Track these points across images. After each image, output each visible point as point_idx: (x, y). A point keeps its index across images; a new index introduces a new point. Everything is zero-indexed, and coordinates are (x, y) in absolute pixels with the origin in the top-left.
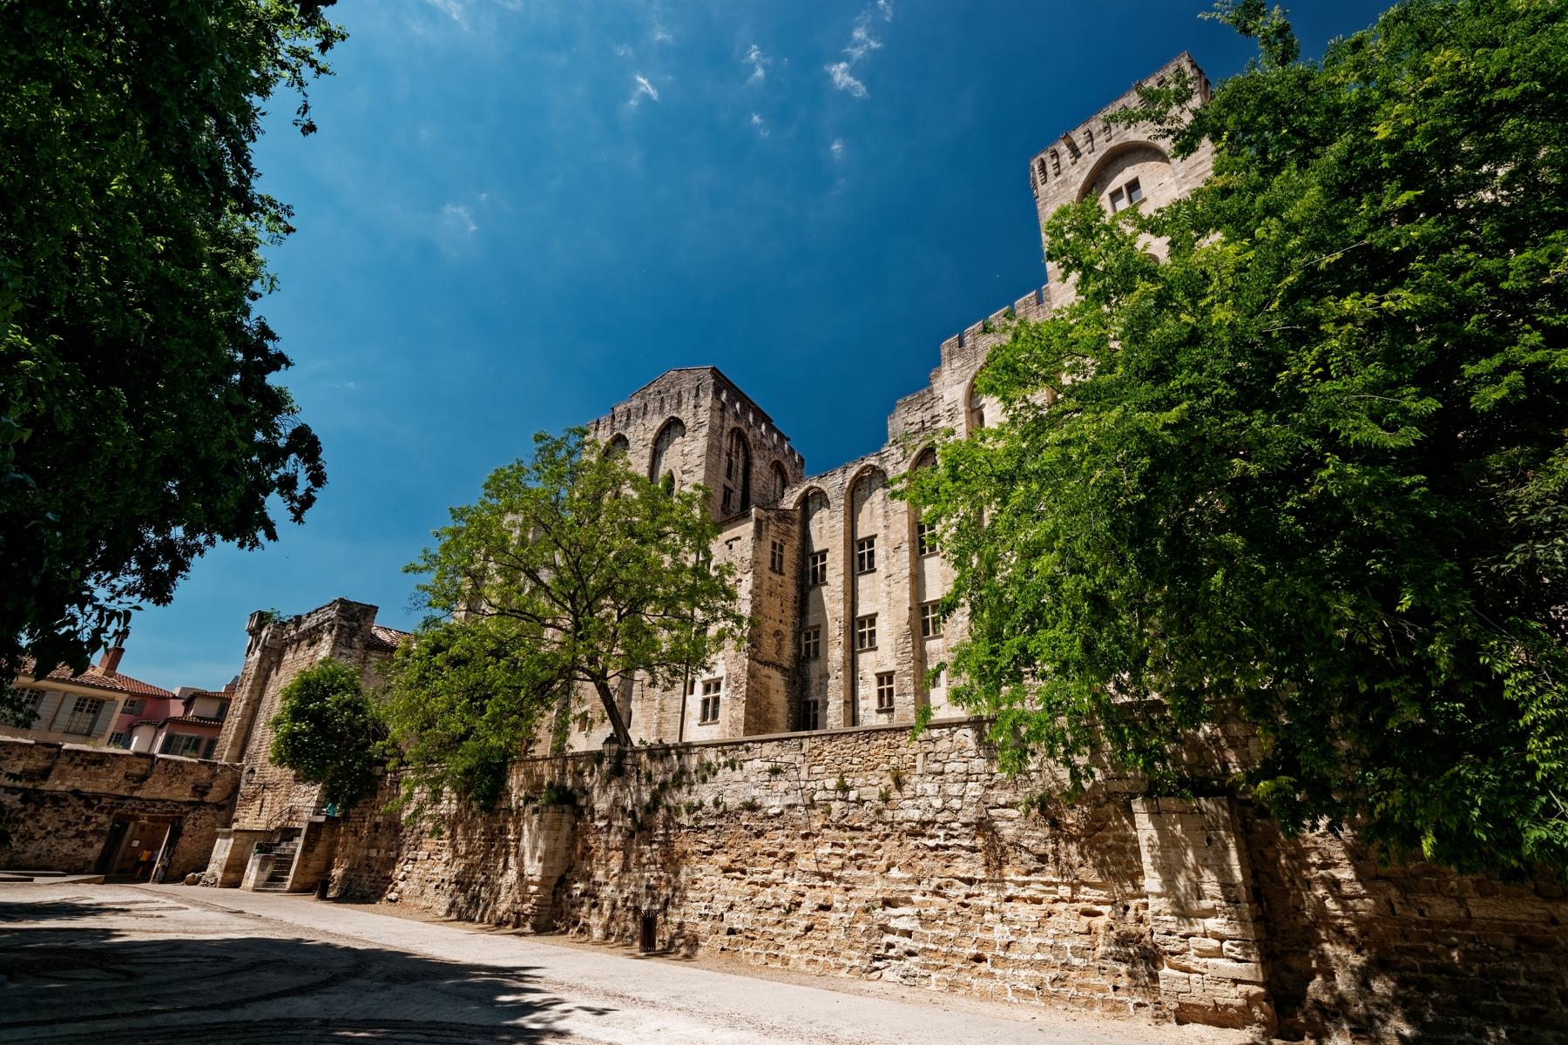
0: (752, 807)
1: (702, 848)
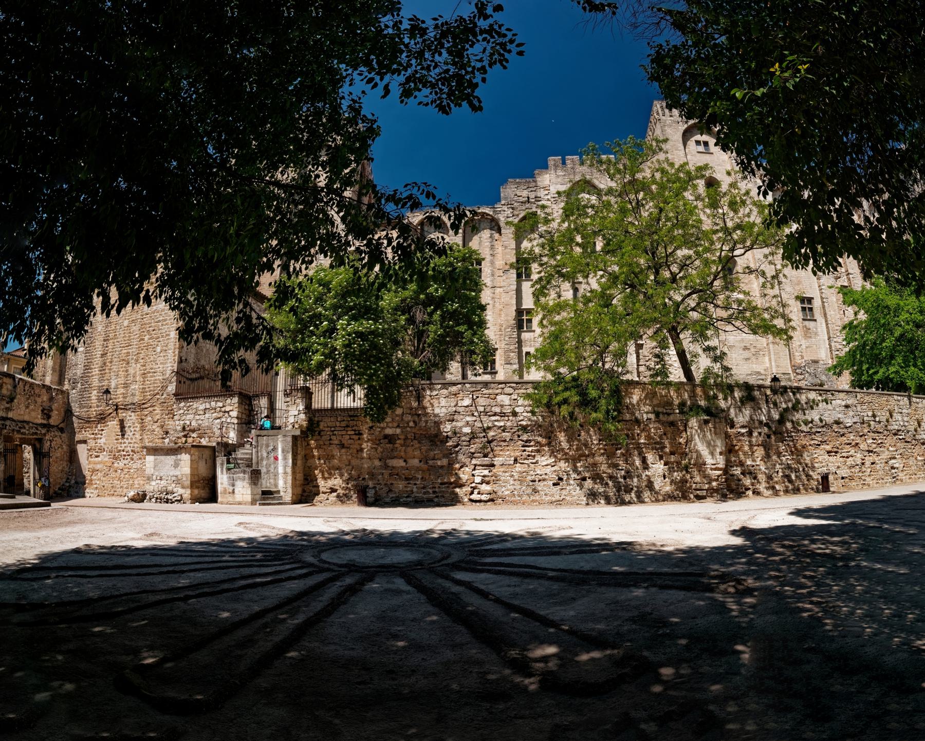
0: (838, 422)
1: (816, 442)
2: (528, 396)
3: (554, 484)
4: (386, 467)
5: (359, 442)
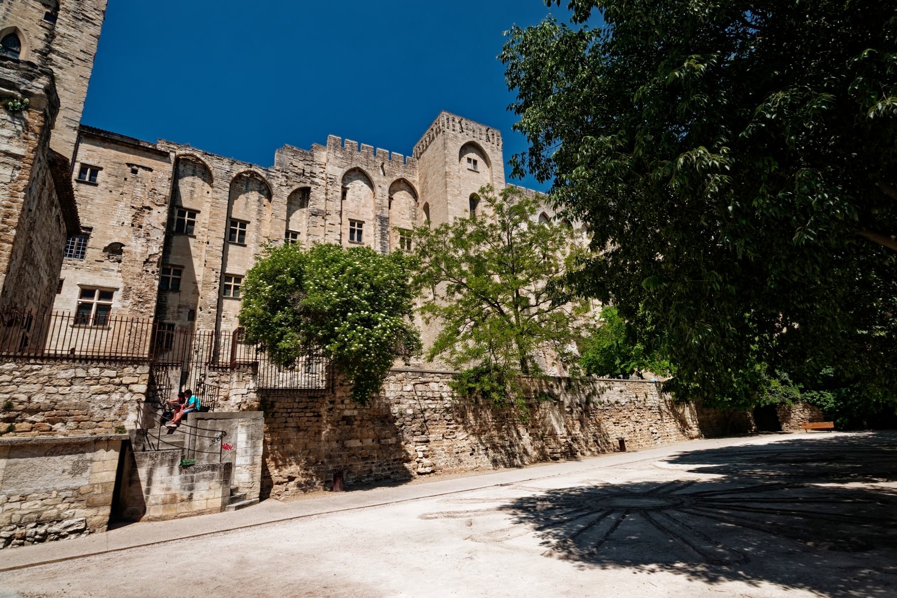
2: (449, 384)
3: (471, 454)
4: (344, 447)
5: (318, 424)
